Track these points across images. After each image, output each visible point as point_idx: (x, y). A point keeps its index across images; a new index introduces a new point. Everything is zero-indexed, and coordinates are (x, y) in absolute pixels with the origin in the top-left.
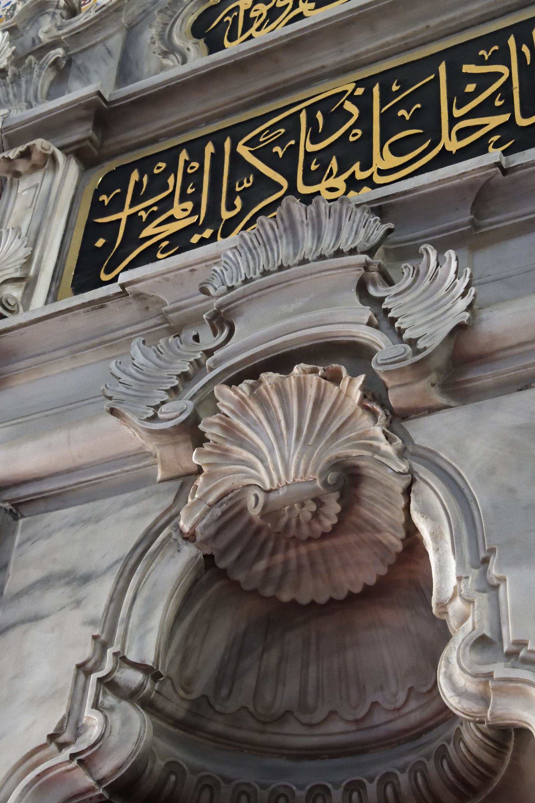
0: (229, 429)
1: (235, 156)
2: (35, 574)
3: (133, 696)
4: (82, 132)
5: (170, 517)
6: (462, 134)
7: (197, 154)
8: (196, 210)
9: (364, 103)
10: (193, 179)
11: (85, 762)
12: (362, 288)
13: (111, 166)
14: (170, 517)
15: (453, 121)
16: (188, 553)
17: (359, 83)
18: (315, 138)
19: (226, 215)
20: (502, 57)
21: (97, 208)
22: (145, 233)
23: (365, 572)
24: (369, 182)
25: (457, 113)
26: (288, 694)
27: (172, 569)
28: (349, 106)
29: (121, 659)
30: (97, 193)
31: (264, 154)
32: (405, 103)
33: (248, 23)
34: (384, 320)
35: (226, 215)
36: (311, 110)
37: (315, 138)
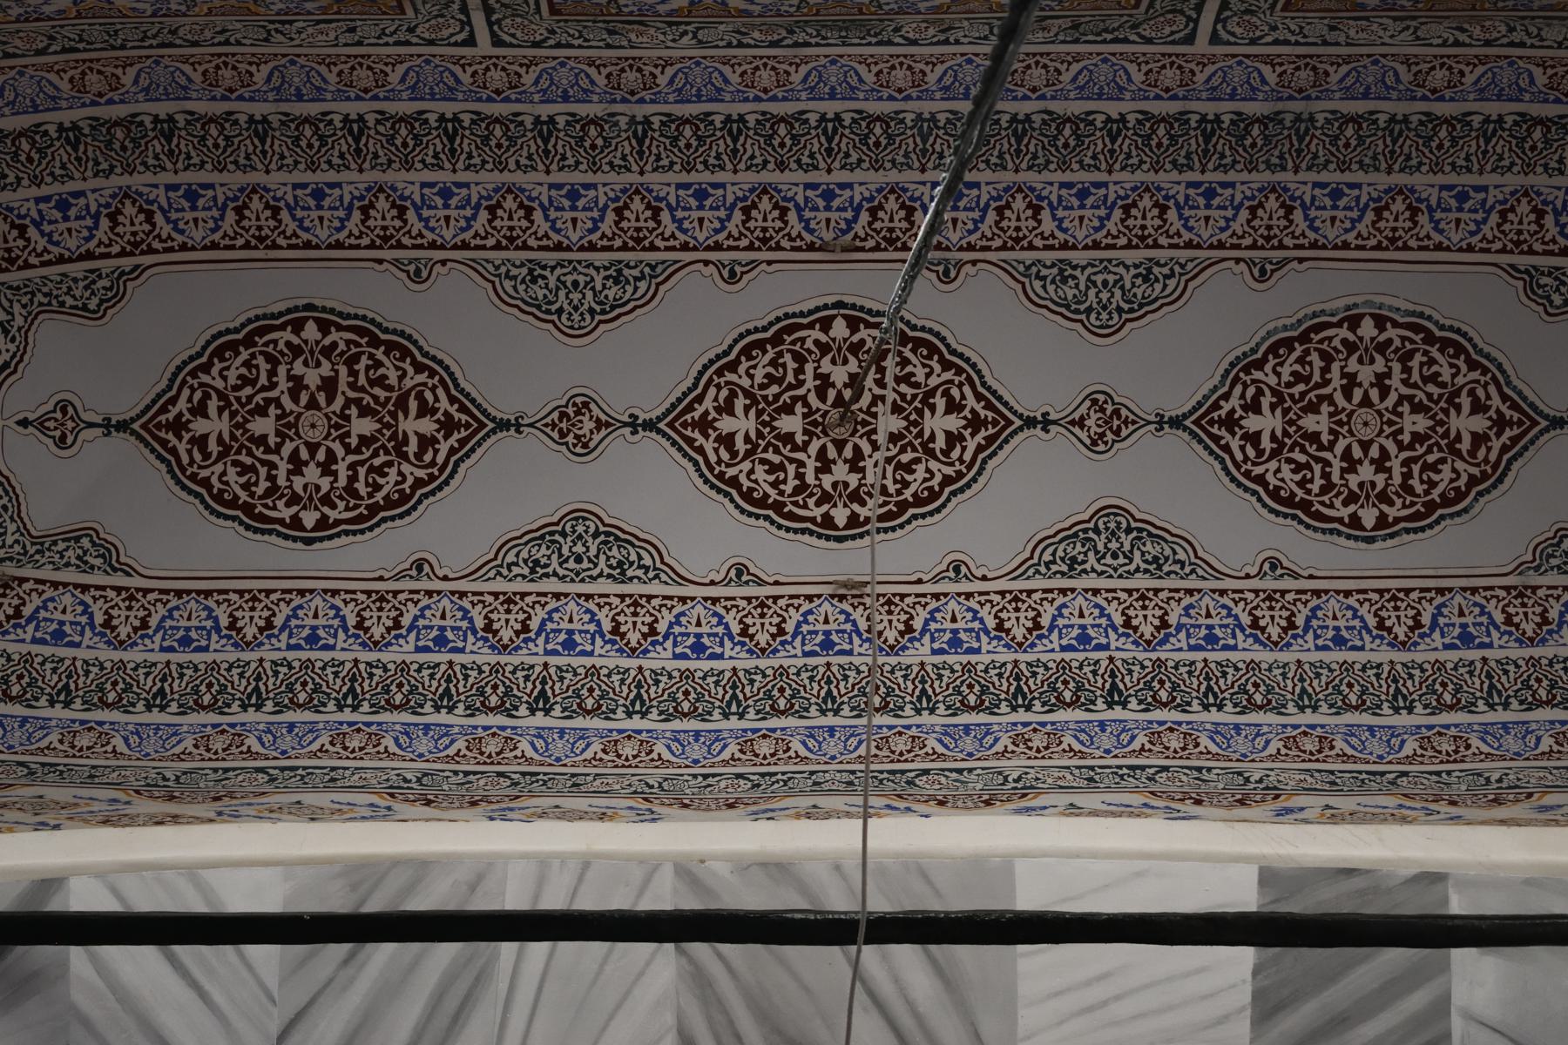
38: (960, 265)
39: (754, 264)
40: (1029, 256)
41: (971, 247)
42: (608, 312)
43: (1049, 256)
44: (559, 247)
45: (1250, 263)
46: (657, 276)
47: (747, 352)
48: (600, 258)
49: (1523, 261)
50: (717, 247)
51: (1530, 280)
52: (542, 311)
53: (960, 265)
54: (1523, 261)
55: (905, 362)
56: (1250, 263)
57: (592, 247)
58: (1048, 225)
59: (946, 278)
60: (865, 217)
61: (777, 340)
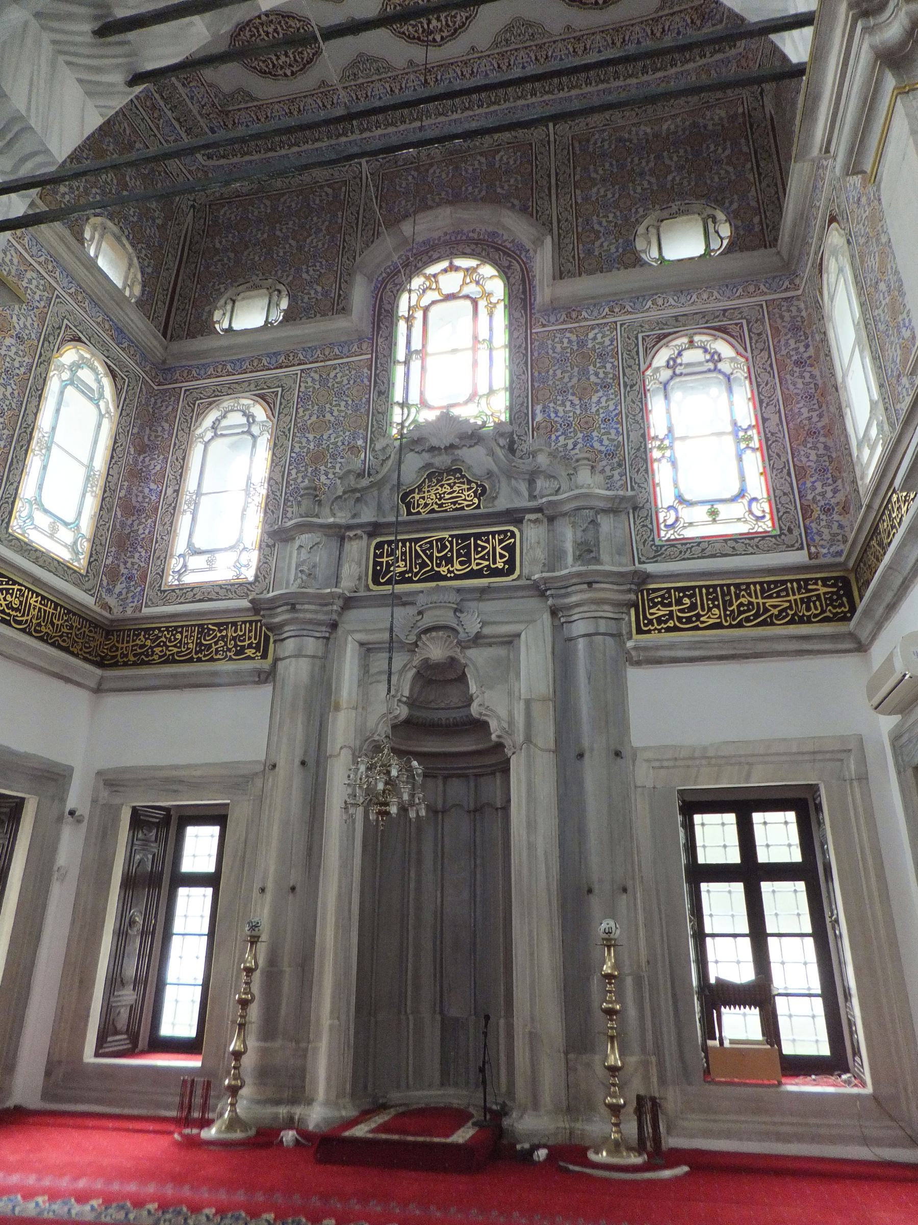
0: (424, 644)
1: (416, 550)
2: (378, 670)
3: (405, 703)
4: (369, 529)
5: (410, 661)
6: (478, 564)
7: (404, 545)
8: (406, 566)
9: (451, 543)
10: (404, 554)
11: (396, 717)
12: (455, 613)
13: (379, 540)
14: (410, 661)
15: (475, 559)
16: (415, 670)
17: (450, 536)
18: (439, 552)
19: (415, 570)
20: (487, 541)
21: (375, 553)
22: (392, 569)
23: (453, 676)
24: (453, 572)
25: (477, 557)
26: (432, 697)
27: (410, 674)
28: (447, 543)
29: (402, 696)
30: (376, 548)
31: (424, 551)
32: (463, 548)
33: (418, 505)
34: (460, 623)
35: (415, 570)
36: (437, 540)
37: (439, 552)
38: (408, 67)
39: (468, 54)
40: (390, 74)
41: (407, 74)
42: (509, 28)
43: (384, 76)
44: (526, 48)
45: (328, 86)
46: (496, 44)
47: (464, 24)
48: (513, 46)
49: (255, 103)
50: (479, 58)
51: (253, 99)
52: (529, 24)
53: (408, 67)
54: (255, 103)
55: (416, 31)
56: (328, 86)
57: (516, 50)
58: (387, 85)
59: (411, 62)
60: (439, 77)
61: (456, 30)
